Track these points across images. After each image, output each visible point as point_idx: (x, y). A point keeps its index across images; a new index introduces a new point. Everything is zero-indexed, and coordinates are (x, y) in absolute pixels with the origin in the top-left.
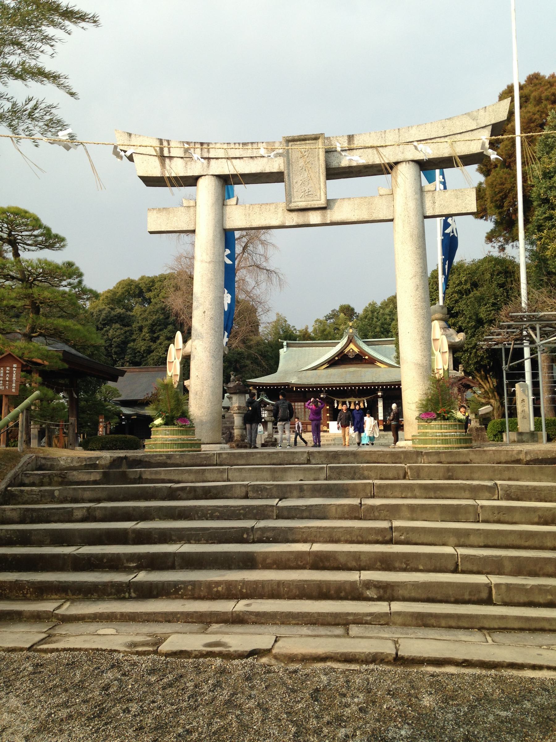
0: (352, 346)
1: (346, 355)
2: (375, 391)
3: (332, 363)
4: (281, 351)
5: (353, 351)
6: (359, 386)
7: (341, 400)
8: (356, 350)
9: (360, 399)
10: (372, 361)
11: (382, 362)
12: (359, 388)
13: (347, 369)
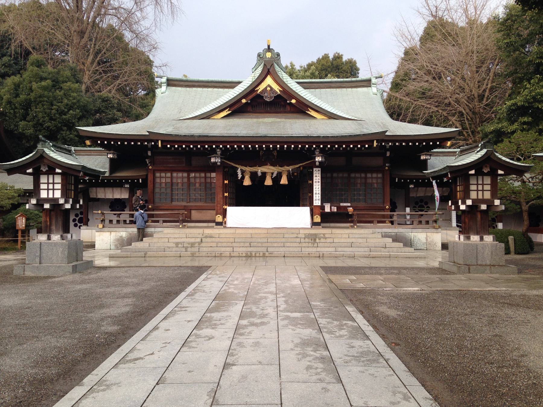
0: (269, 81)
1: (259, 97)
2: (311, 155)
3: (236, 108)
4: (158, 91)
5: (272, 88)
6: (282, 143)
7: (248, 169)
8: (276, 88)
9: (280, 169)
10: (302, 109)
11: (318, 110)
12: (282, 147)
13: (261, 120)
